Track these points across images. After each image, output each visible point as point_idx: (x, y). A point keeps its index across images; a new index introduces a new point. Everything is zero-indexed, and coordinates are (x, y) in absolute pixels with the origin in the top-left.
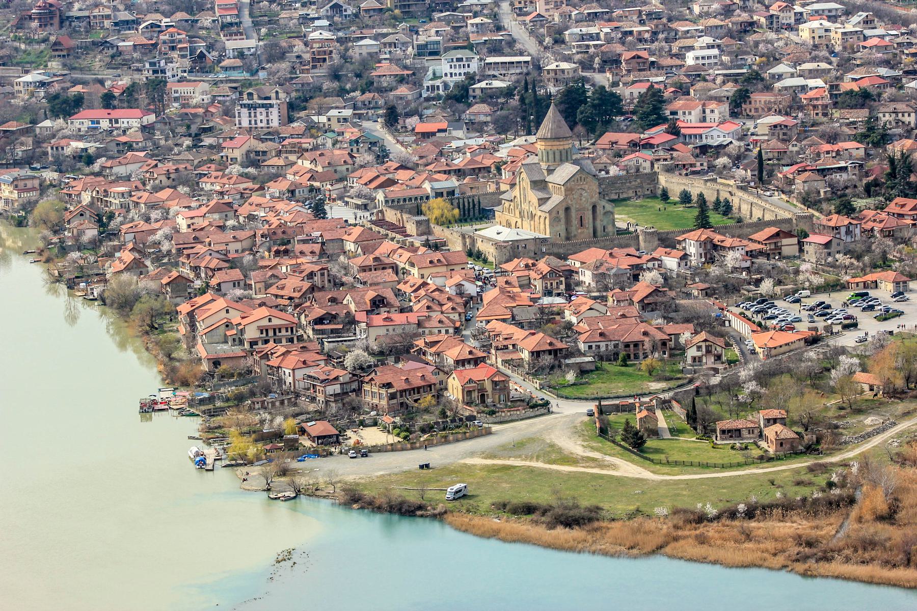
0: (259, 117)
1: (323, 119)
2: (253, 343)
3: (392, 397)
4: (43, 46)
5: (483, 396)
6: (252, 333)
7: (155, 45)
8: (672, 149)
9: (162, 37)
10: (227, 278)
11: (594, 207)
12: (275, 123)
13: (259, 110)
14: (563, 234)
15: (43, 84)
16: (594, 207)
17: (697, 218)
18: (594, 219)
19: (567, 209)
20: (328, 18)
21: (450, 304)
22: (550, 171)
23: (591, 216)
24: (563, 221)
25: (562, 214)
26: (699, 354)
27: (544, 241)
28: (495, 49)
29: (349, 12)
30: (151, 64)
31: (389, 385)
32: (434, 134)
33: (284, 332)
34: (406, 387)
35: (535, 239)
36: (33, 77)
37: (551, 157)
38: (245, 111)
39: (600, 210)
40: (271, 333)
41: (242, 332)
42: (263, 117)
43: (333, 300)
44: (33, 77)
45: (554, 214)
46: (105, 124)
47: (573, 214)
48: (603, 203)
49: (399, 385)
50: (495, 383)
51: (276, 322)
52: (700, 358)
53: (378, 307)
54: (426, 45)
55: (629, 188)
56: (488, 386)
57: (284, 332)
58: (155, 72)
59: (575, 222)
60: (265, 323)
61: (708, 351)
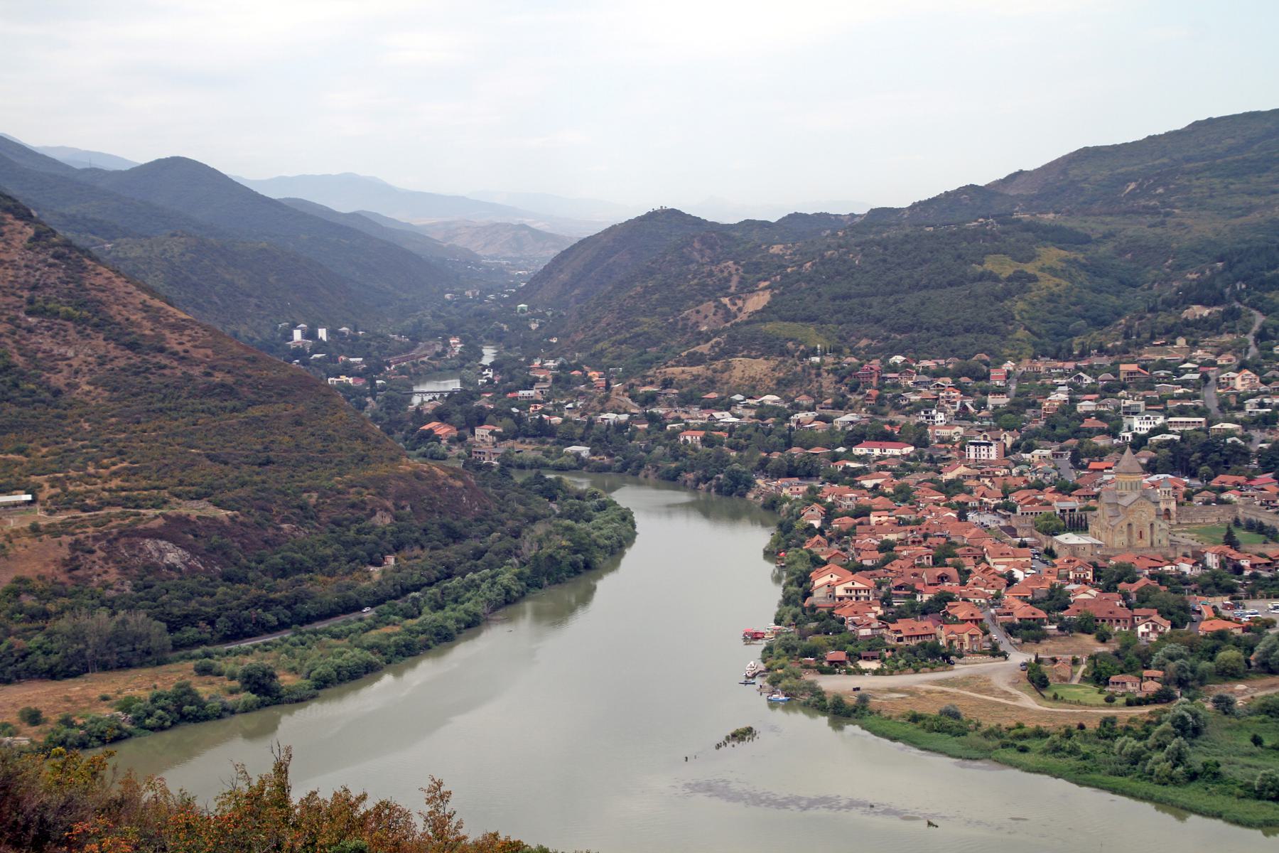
0: (982, 452)
1: (1028, 456)
2: (841, 598)
3: (900, 639)
4: (861, 397)
5: (962, 644)
6: (840, 591)
7: (937, 399)
8: (1263, 489)
9: (941, 394)
10: (867, 557)
11: (1152, 525)
12: (994, 457)
13: (982, 447)
14: (1126, 543)
15: (852, 422)
16: (1152, 525)
17: (1226, 537)
18: (1152, 533)
19: (1130, 525)
20: (1070, 385)
21: (994, 583)
22: (1122, 496)
23: (1149, 532)
24: (1126, 533)
25: (1125, 529)
26: (1147, 630)
27: (1099, 546)
28: (1182, 412)
29: (1088, 382)
30: (926, 412)
31: (899, 631)
32: (1102, 470)
33: (862, 593)
34: (912, 633)
35: (1092, 544)
36: (850, 417)
37: (1124, 486)
38: (972, 448)
39: (1156, 528)
40: (854, 593)
41: (834, 590)
42: (985, 452)
43: (915, 575)
44: (850, 417)
45: (1118, 528)
46: (877, 452)
47: (1134, 528)
48: (1159, 522)
49: (905, 633)
50: (971, 636)
51: (857, 585)
52: (1148, 634)
53: (943, 581)
54: (1129, 407)
55: (1213, 516)
56: (966, 637)
57: (862, 593)
58: (927, 418)
59: (1136, 535)
60: (849, 585)
61: (1154, 627)
